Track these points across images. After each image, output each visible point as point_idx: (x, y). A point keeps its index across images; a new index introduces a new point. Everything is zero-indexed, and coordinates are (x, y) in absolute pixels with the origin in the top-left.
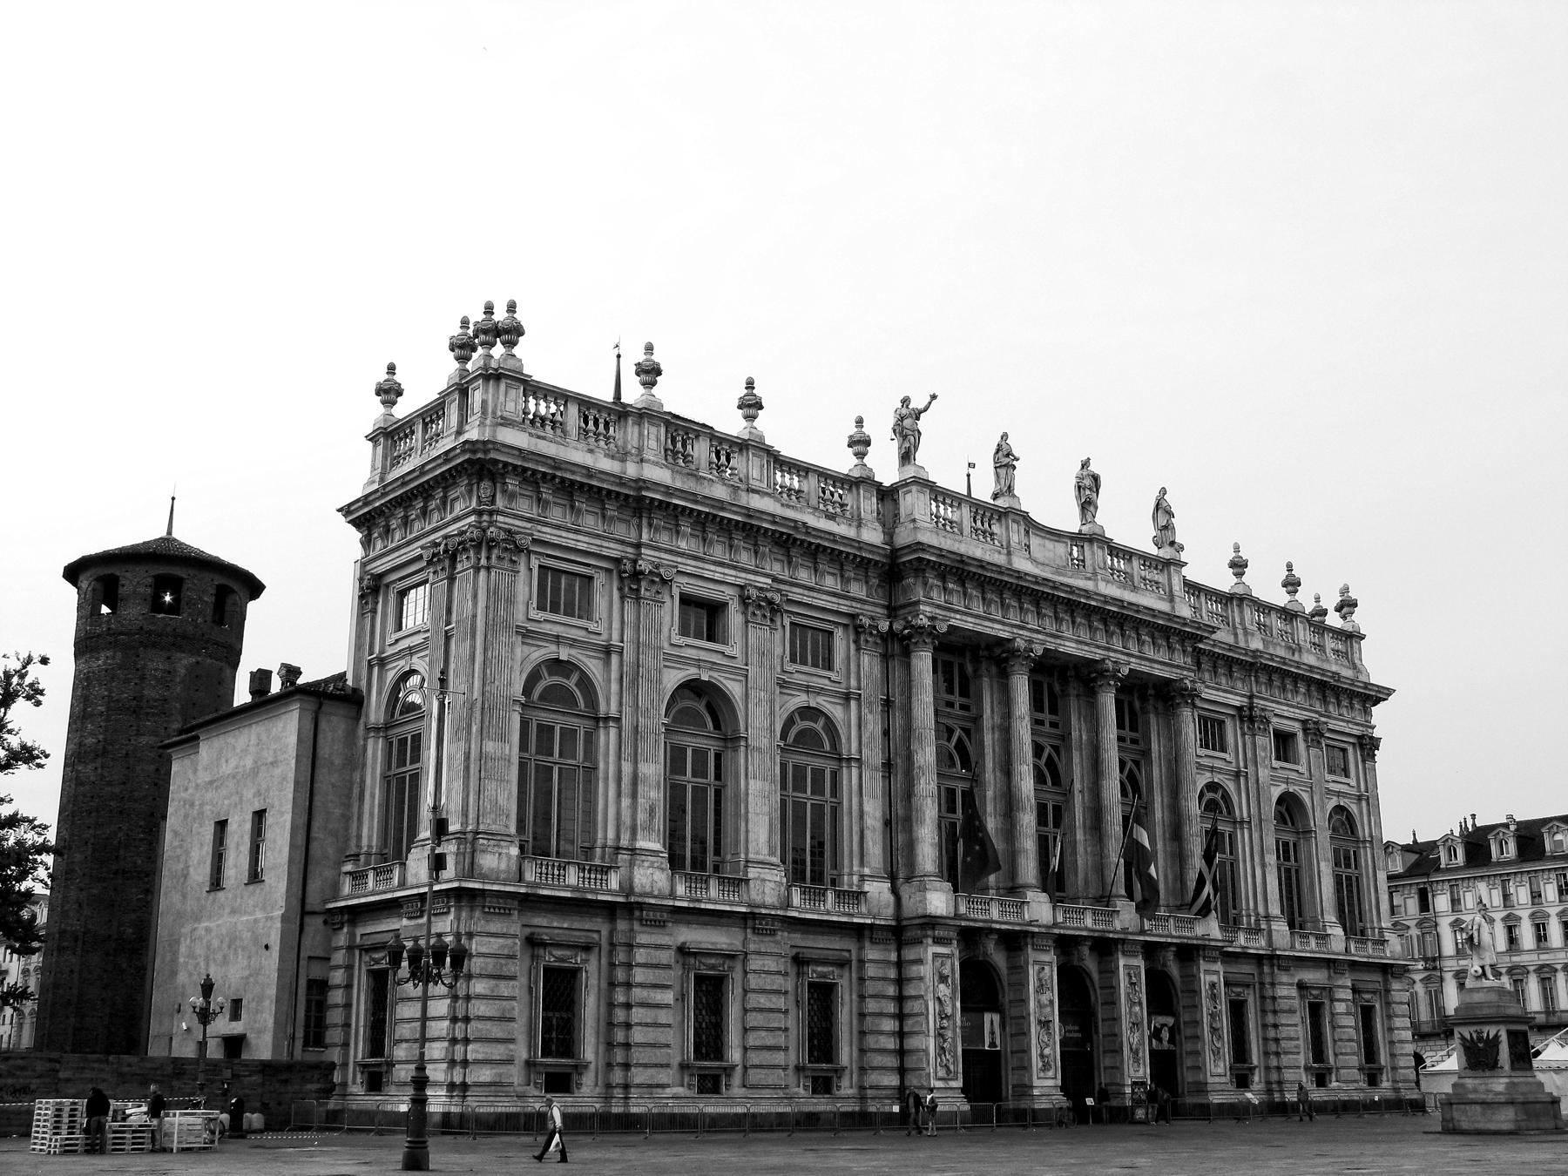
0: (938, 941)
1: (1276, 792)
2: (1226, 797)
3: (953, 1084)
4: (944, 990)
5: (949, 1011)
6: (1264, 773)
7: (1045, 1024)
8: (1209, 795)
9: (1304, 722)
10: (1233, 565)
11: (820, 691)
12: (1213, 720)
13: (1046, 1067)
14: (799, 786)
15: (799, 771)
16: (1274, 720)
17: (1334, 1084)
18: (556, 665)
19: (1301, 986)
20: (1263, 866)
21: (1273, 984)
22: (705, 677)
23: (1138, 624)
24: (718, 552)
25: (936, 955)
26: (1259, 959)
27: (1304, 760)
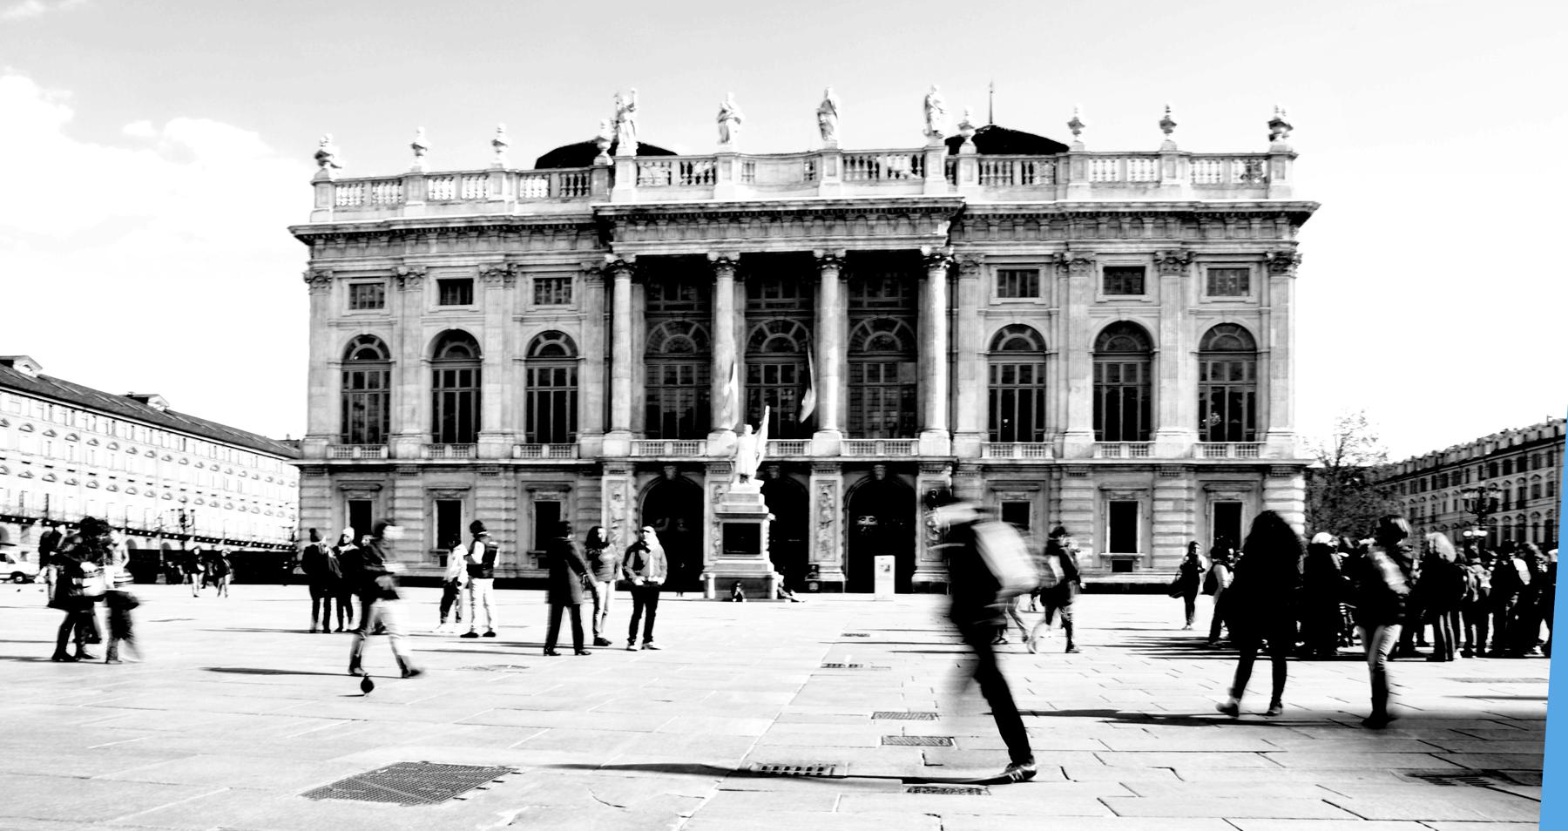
0: (613, 472)
2: (1036, 335)
4: (614, 503)
5: (618, 517)
6: (1078, 310)
8: (1009, 336)
9: (1154, 254)
14: (544, 381)
15: (544, 373)
16: (1099, 258)
18: (365, 339)
19: (1102, 490)
20: (1069, 390)
21: (1060, 489)
22: (454, 327)
23: (861, 214)
26: (1049, 468)
27: (1155, 292)
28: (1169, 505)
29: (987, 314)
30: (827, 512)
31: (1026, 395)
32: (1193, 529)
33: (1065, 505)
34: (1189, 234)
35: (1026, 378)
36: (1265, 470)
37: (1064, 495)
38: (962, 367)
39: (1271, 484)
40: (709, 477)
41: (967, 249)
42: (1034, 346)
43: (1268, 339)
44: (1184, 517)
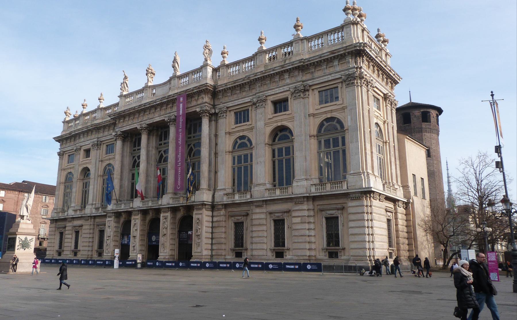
0: (110, 217)
1: (269, 130)
2: (249, 140)
3: (109, 254)
6: (260, 124)
7: (134, 237)
8: (239, 142)
10: (259, 40)
11: (110, 159)
12: (244, 111)
13: (134, 250)
16: (269, 98)
17: (288, 257)
19: (270, 213)
24: (89, 138)
25: (109, 221)
28: (298, 220)
29: (230, 133)
30: (164, 230)
31: (246, 168)
32: (312, 233)
33: (255, 222)
34: (309, 76)
35: (246, 161)
36: (346, 195)
37: (255, 217)
38: (220, 159)
39: (351, 204)
40: (133, 217)
41: (221, 106)
42: (249, 145)
43: (348, 123)
44: (307, 226)
